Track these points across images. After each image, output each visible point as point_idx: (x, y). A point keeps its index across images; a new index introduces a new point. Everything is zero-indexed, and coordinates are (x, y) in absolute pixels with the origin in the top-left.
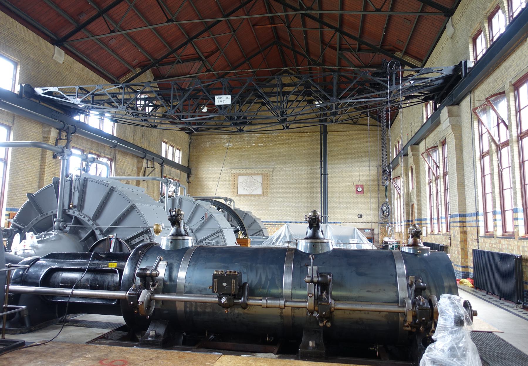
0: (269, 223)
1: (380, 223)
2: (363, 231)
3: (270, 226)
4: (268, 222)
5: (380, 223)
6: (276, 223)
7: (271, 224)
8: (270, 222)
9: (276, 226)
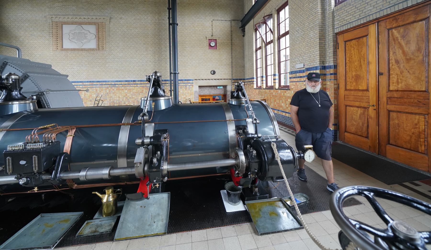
0: (107, 83)
2: (216, 88)
3: (108, 86)
4: (106, 81)
6: (117, 83)
7: (110, 83)
8: (109, 81)
9: (117, 86)
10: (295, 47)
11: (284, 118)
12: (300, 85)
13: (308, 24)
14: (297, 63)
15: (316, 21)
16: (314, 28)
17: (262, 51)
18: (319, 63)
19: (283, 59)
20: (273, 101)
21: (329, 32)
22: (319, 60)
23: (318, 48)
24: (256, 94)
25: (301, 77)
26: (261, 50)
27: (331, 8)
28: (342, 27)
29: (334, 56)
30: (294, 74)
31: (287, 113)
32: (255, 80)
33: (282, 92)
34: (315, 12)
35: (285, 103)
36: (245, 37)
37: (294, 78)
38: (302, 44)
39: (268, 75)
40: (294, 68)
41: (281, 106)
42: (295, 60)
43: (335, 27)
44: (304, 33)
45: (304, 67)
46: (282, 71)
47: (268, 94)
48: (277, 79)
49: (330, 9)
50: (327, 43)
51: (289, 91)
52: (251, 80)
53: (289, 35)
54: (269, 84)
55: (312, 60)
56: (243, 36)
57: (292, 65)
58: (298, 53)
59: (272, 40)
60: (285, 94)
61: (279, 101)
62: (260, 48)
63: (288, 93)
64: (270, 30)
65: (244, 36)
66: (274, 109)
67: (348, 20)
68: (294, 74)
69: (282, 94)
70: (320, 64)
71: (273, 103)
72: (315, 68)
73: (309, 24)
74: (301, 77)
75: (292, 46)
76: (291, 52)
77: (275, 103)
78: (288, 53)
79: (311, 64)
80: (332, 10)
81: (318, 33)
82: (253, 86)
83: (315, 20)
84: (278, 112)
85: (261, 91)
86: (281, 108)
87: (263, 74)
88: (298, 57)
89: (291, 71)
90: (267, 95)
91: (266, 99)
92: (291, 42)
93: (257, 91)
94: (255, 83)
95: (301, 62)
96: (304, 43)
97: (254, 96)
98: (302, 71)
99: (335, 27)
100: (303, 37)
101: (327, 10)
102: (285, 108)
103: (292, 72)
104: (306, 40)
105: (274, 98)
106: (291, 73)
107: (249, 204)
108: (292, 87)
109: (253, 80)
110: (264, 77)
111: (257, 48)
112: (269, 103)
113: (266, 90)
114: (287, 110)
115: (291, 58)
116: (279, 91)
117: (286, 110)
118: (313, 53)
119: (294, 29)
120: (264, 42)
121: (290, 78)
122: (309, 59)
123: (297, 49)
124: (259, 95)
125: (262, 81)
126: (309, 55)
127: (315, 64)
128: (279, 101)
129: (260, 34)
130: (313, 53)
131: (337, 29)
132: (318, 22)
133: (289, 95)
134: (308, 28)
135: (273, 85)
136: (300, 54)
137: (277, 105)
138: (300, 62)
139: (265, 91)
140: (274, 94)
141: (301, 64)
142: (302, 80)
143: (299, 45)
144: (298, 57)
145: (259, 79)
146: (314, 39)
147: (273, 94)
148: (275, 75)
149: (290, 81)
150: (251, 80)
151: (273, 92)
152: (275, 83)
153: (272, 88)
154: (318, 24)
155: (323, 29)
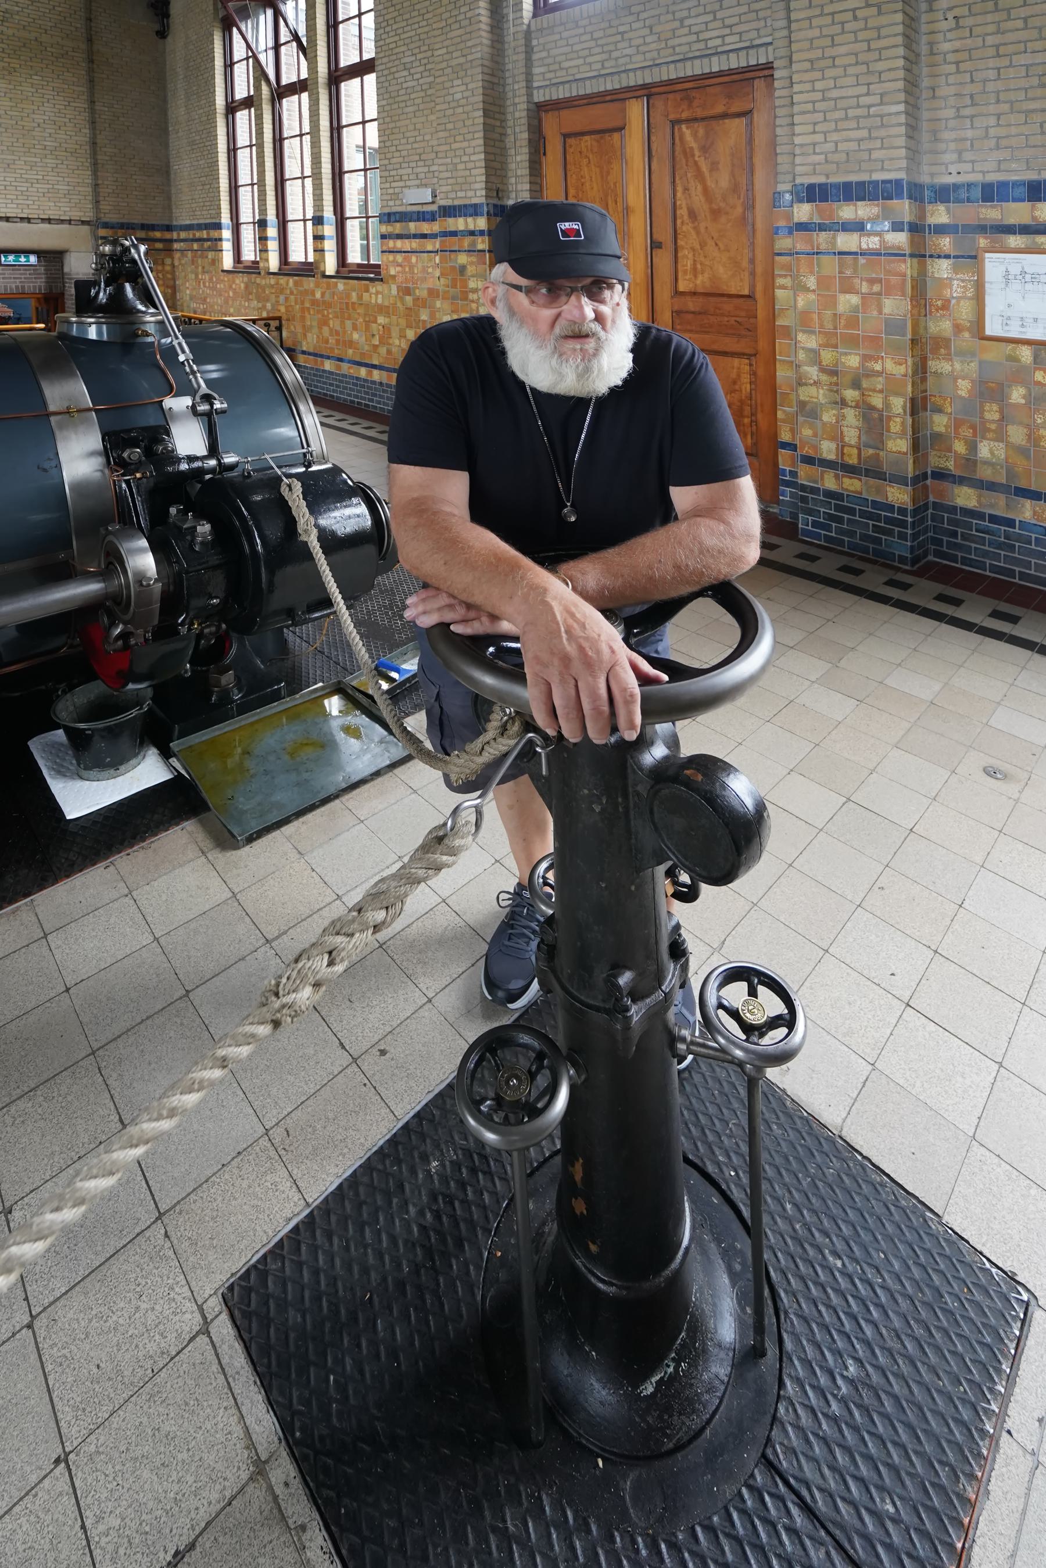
1: (106, 225)
5: (106, 225)
10: (398, 124)
11: (363, 386)
12: (420, 265)
13: (444, 51)
14: (408, 183)
15: (473, 50)
16: (466, 70)
17: (259, 118)
18: (484, 193)
19: (353, 160)
20: (315, 323)
21: (514, 96)
22: (483, 185)
23: (481, 142)
24: (235, 292)
25: (424, 236)
26: (253, 110)
27: (522, 17)
28: (554, 89)
29: (531, 175)
30: (396, 221)
31: (374, 367)
32: (227, 234)
33: (354, 290)
34: (470, 19)
35: (367, 328)
36: (169, 39)
37: (399, 237)
38: (423, 119)
39: (290, 216)
40: (398, 202)
41: (351, 344)
42: (400, 172)
43: (535, 84)
44: (431, 79)
45: (433, 203)
46: (352, 207)
47: (292, 293)
48: (331, 238)
49: (519, 21)
50: (509, 131)
51: (379, 286)
52: (204, 234)
53: (377, 78)
54: (297, 255)
55: (460, 180)
56: (157, 33)
57: (391, 191)
58: (409, 147)
59: (306, 79)
60: (366, 296)
61: (342, 323)
62: (248, 102)
63: (377, 293)
64: (296, 37)
65: (162, 34)
66: (322, 356)
67: (570, 71)
68: (398, 225)
69: (354, 294)
70: (487, 197)
71: (315, 330)
72: (471, 210)
73: (448, 53)
74: (424, 236)
75: (388, 120)
76: (384, 142)
77: (326, 331)
78: (373, 140)
79: (460, 194)
80: (525, 27)
81: (481, 91)
82: (217, 261)
83: (469, 44)
84: (339, 368)
85: (258, 280)
86: (350, 352)
87: (263, 210)
88: (413, 164)
89: (387, 210)
90: (287, 299)
91: (284, 317)
92: (384, 103)
93: (240, 281)
94: (227, 246)
95: (424, 182)
96: (432, 117)
97: (226, 302)
98: (427, 216)
99: (535, 84)
100: (429, 92)
101: (508, 21)
102: (366, 348)
103: (389, 214)
104: (438, 108)
105: (318, 312)
106: (387, 218)
107: (190, 747)
108: (392, 272)
109: (214, 234)
110: (269, 223)
111: (233, 101)
112: (299, 330)
113: (283, 280)
114: (375, 355)
115: (386, 162)
116: (341, 285)
117: (371, 356)
118: (465, 158)
119: (394, 57)
120: (268, 80)
121: (383, 237)
122: (449, 175)
123: (408, 134)
124: (249, 300)
125: (263, 239)
126: (449, 160)
127: (470, 194)
128: (342, 323)
129: (249, 47)
130: (465, 158)
131: (541, 91)
132: (479, 55)
133: (380, 301)
134: (444, 65)
135: (311, 259)
136: (418, 151)
137: (332, 341)
138: (418, 182)
139: (277, 284)
140: (318, 295)
141: (422, 190)
142: (430, 248)
143: (414, 120)
144: (413, 164)
145: (248, 234)
146: (467, 109)
147: (314, 295)
148: (318, 220)
149: (385, 248)
150: (204, 234)
151: (312, 285)
152: (323, 251)
153: (307, 270)
154: (480, 62)
155: (496, 81)
